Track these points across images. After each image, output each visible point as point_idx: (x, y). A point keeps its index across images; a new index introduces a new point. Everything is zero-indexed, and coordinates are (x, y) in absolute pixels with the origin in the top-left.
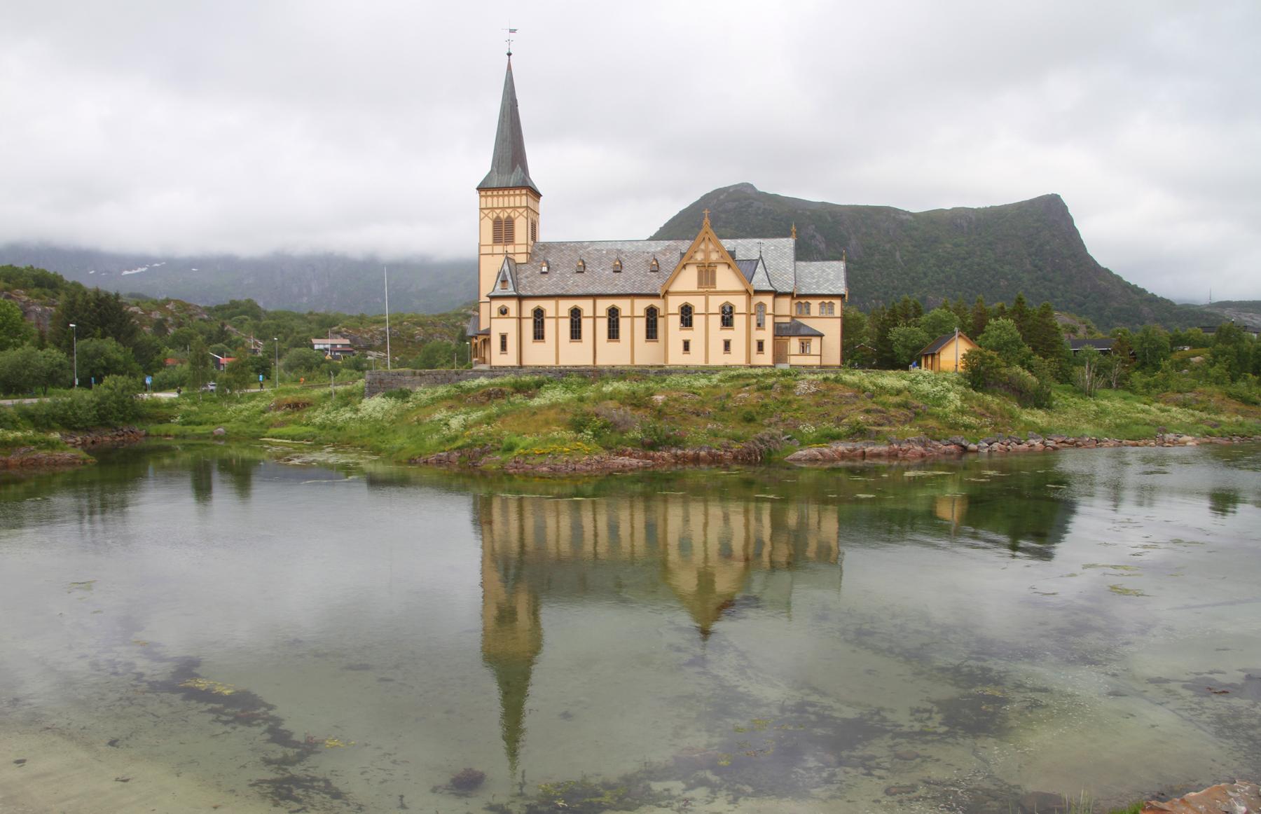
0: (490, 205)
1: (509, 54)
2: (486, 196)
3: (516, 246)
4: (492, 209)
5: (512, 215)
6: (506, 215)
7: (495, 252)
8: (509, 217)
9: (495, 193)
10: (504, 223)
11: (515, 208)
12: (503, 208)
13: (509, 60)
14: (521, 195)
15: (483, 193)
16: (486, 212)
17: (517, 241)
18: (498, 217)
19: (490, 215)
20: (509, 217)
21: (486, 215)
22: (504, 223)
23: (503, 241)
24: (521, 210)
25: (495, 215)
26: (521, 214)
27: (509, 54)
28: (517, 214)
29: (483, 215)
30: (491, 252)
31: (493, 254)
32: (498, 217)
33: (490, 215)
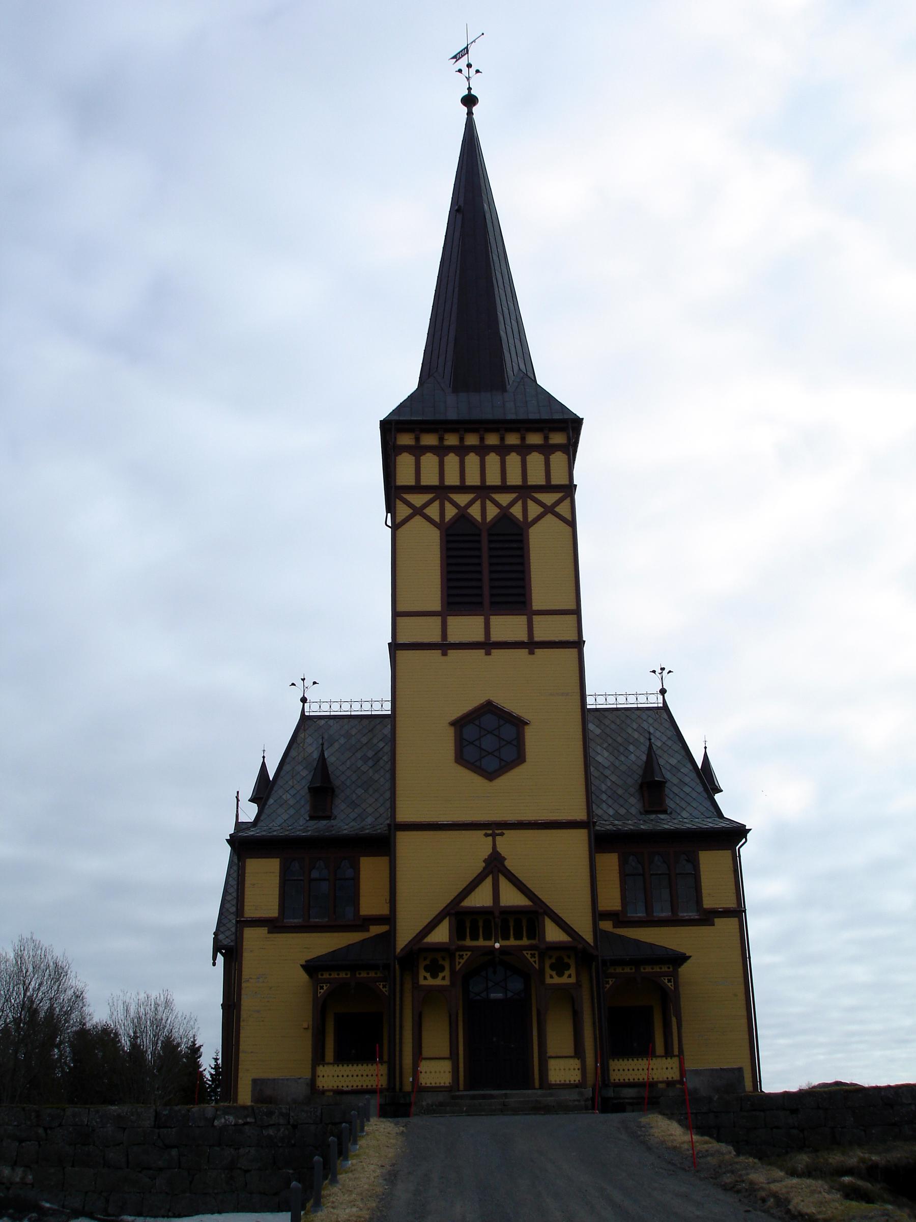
0: (430, 478)
1: (469, 101)
2: (418, 451)
3: (536, 619)
4: (441, 491)
5: (517, 511)
6: (492, 512)
7: (452, 639)
8: (505, 515)
9: (452, 440)
10: (485, 539)
11: (525, 491)
12: (483, 491)
13: (470, 113)
14: (546, 450)
15: (405, 439)
16: (418, 500)
17: (536, 606)
18: (463, 516)
19: (433, 511)
20: (505, 515)
21: (418, 511)
22: (485, 539)
23: (486, 600)
24: (548, 498)
25: (451, 512)
26: (549, 510)
27: (469, 101)
28: (534, 510)
29: (403, 511)
30: (436, 638)
31: (444, 647)
32: (463, 516)
33: (433, 511)
